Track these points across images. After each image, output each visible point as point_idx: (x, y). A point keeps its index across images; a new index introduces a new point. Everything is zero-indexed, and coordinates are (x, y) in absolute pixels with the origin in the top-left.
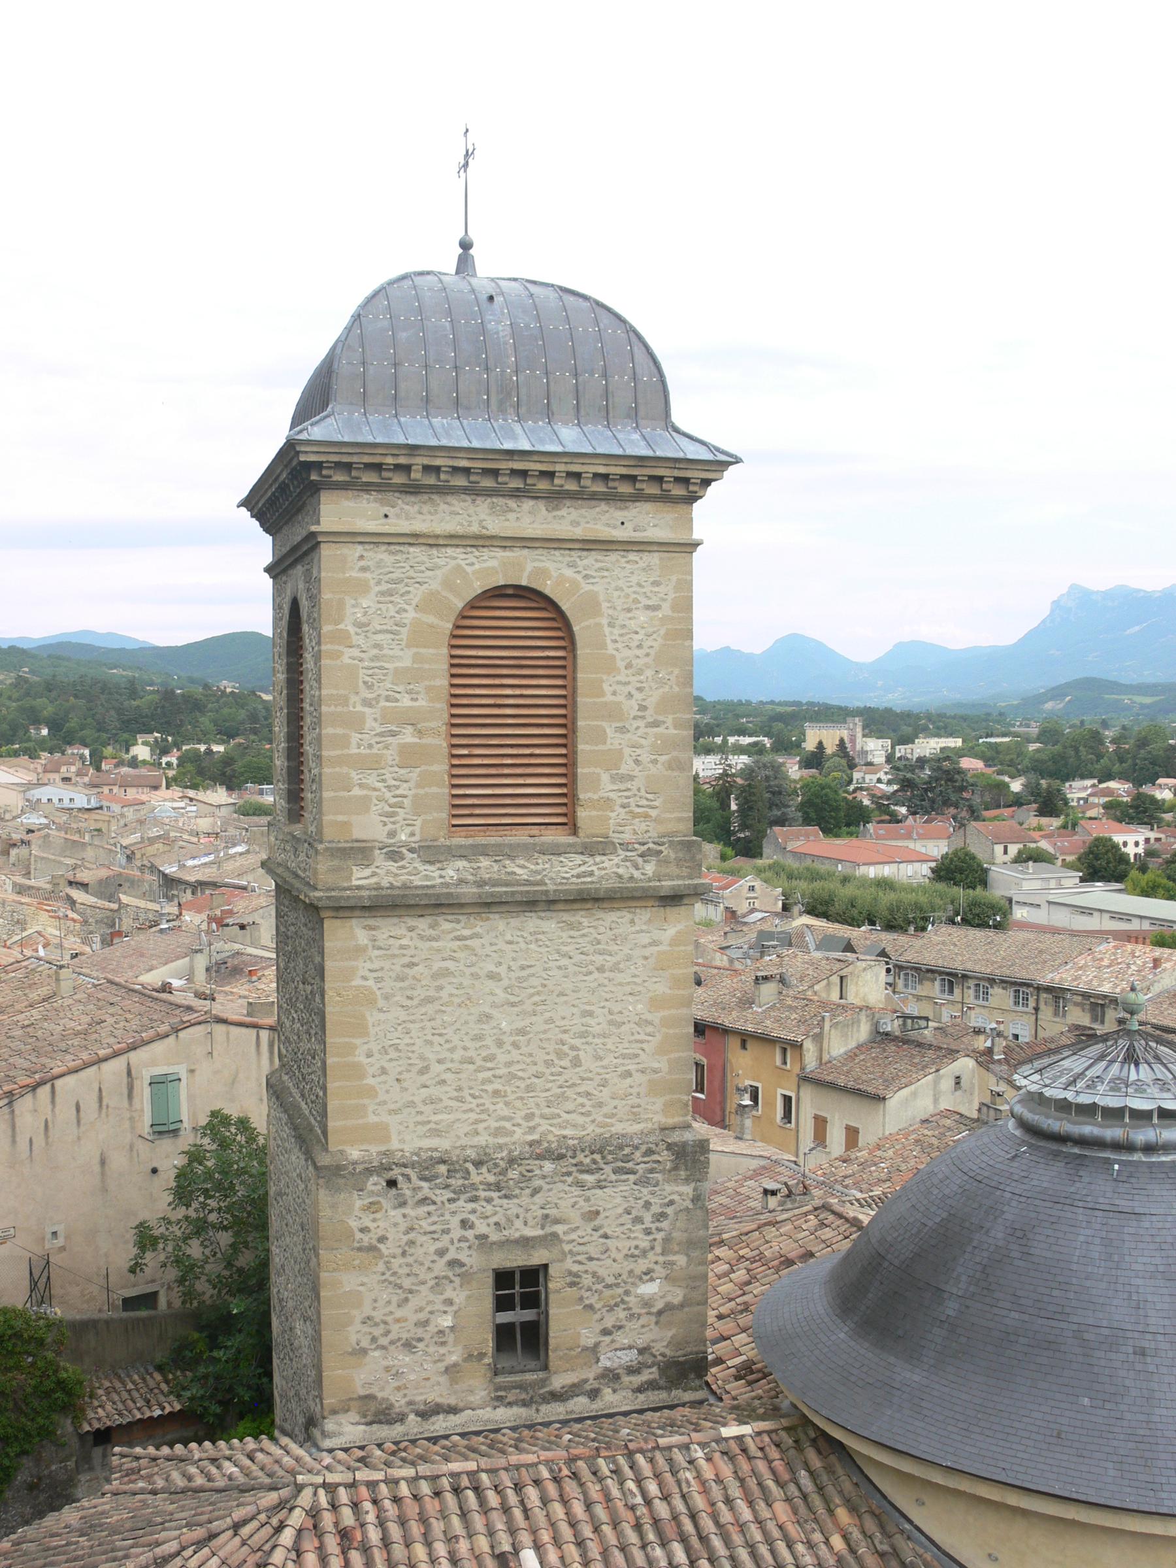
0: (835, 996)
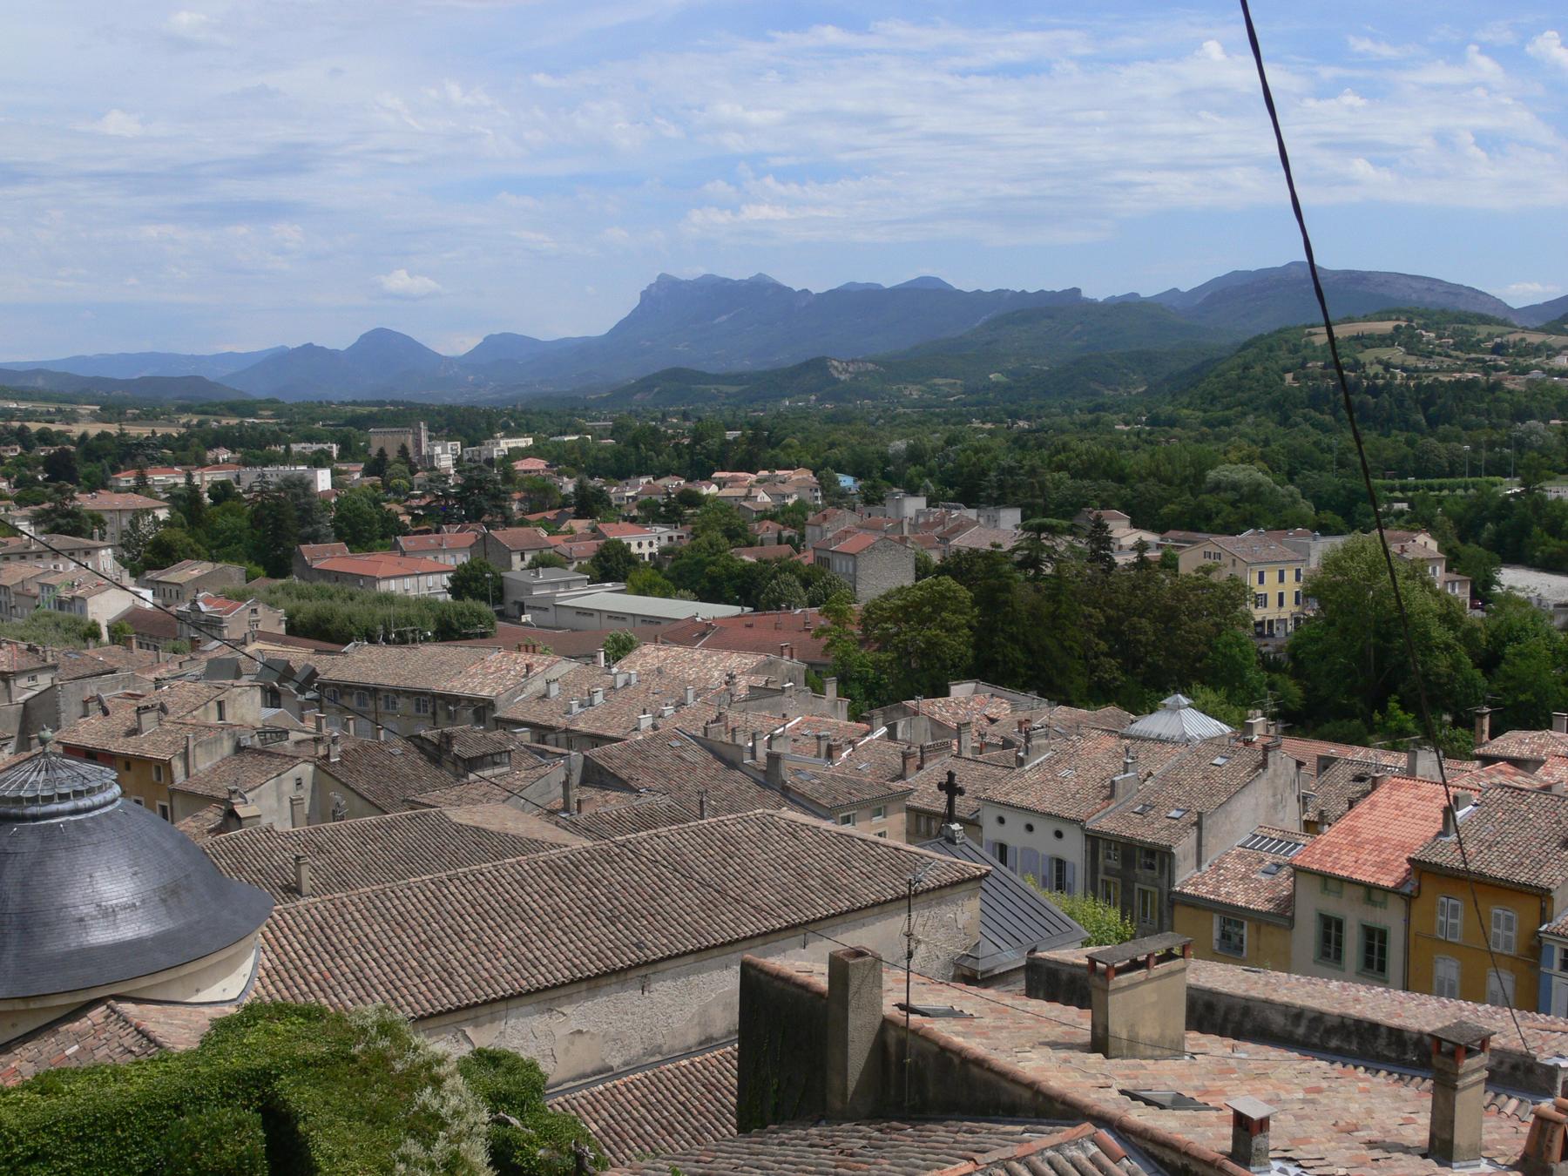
0: (213, 719)
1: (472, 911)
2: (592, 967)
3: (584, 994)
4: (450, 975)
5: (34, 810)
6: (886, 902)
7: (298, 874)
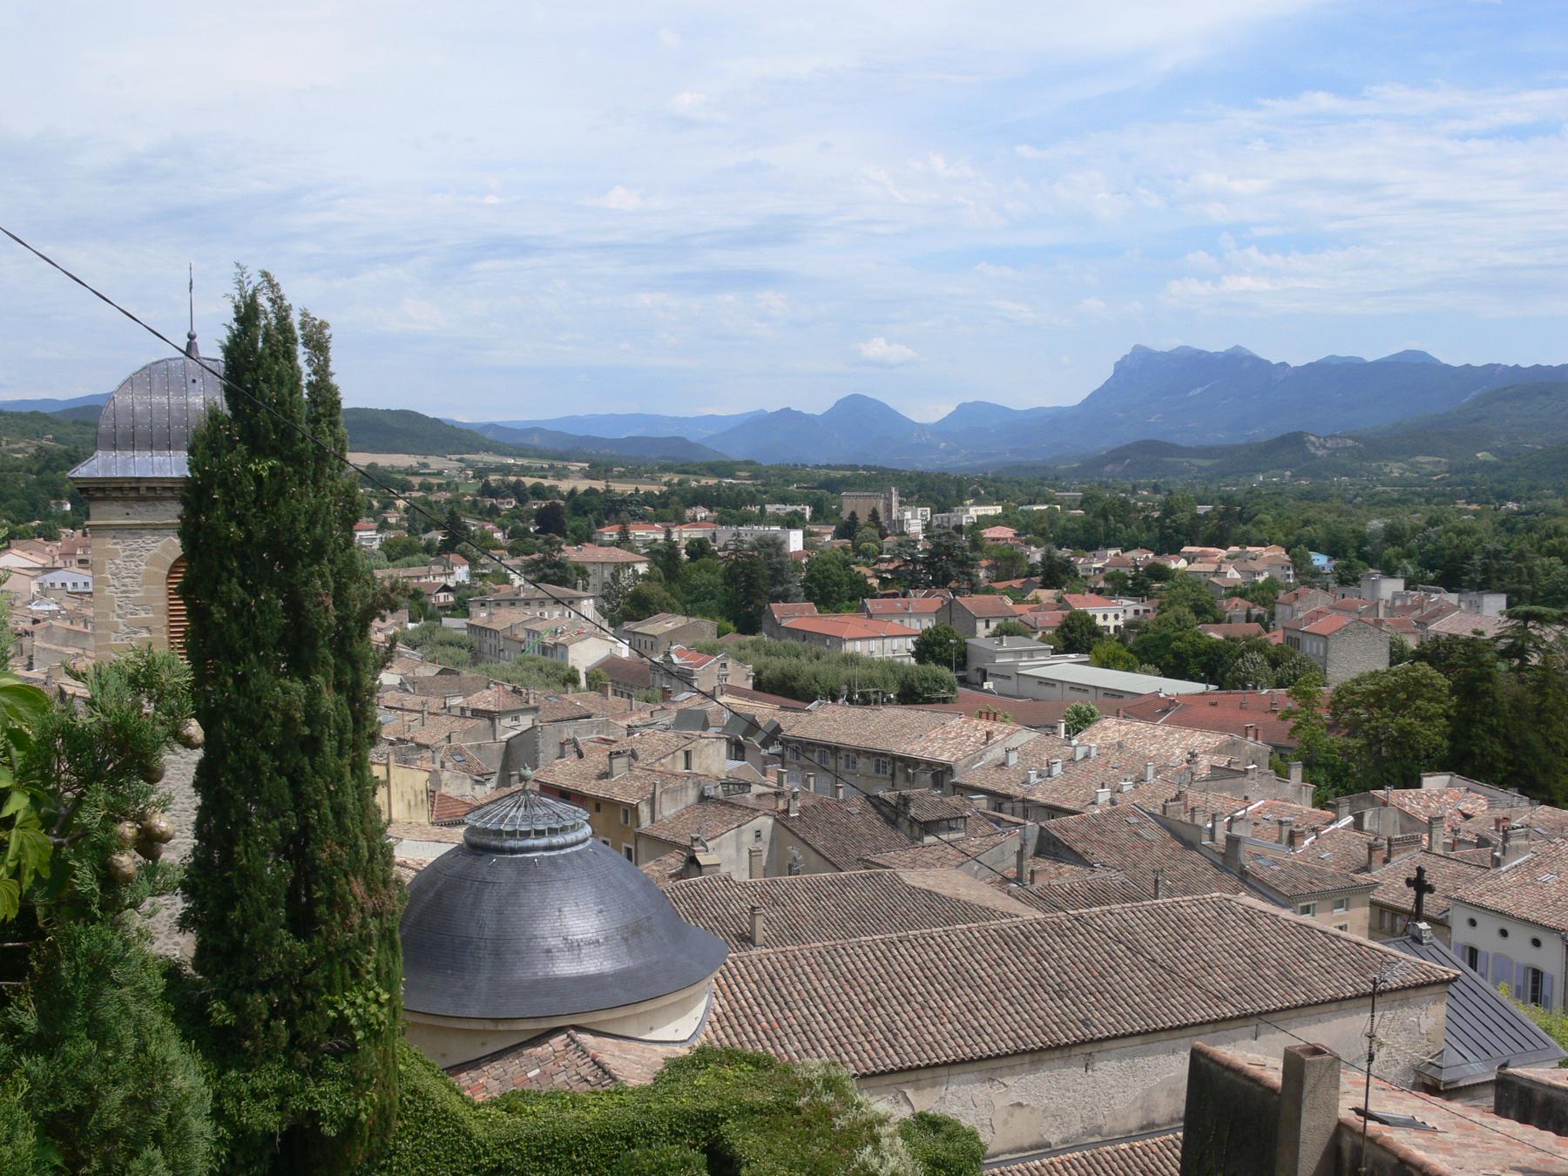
0: (680, 767)
1: (920, 974)
2: (1036, 1040)
3: (1027, 1066)
4: (895, 1035)
5: (512, 843)
6: (1344, 999)
7: (752, 924)
